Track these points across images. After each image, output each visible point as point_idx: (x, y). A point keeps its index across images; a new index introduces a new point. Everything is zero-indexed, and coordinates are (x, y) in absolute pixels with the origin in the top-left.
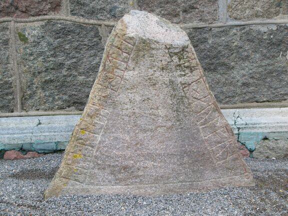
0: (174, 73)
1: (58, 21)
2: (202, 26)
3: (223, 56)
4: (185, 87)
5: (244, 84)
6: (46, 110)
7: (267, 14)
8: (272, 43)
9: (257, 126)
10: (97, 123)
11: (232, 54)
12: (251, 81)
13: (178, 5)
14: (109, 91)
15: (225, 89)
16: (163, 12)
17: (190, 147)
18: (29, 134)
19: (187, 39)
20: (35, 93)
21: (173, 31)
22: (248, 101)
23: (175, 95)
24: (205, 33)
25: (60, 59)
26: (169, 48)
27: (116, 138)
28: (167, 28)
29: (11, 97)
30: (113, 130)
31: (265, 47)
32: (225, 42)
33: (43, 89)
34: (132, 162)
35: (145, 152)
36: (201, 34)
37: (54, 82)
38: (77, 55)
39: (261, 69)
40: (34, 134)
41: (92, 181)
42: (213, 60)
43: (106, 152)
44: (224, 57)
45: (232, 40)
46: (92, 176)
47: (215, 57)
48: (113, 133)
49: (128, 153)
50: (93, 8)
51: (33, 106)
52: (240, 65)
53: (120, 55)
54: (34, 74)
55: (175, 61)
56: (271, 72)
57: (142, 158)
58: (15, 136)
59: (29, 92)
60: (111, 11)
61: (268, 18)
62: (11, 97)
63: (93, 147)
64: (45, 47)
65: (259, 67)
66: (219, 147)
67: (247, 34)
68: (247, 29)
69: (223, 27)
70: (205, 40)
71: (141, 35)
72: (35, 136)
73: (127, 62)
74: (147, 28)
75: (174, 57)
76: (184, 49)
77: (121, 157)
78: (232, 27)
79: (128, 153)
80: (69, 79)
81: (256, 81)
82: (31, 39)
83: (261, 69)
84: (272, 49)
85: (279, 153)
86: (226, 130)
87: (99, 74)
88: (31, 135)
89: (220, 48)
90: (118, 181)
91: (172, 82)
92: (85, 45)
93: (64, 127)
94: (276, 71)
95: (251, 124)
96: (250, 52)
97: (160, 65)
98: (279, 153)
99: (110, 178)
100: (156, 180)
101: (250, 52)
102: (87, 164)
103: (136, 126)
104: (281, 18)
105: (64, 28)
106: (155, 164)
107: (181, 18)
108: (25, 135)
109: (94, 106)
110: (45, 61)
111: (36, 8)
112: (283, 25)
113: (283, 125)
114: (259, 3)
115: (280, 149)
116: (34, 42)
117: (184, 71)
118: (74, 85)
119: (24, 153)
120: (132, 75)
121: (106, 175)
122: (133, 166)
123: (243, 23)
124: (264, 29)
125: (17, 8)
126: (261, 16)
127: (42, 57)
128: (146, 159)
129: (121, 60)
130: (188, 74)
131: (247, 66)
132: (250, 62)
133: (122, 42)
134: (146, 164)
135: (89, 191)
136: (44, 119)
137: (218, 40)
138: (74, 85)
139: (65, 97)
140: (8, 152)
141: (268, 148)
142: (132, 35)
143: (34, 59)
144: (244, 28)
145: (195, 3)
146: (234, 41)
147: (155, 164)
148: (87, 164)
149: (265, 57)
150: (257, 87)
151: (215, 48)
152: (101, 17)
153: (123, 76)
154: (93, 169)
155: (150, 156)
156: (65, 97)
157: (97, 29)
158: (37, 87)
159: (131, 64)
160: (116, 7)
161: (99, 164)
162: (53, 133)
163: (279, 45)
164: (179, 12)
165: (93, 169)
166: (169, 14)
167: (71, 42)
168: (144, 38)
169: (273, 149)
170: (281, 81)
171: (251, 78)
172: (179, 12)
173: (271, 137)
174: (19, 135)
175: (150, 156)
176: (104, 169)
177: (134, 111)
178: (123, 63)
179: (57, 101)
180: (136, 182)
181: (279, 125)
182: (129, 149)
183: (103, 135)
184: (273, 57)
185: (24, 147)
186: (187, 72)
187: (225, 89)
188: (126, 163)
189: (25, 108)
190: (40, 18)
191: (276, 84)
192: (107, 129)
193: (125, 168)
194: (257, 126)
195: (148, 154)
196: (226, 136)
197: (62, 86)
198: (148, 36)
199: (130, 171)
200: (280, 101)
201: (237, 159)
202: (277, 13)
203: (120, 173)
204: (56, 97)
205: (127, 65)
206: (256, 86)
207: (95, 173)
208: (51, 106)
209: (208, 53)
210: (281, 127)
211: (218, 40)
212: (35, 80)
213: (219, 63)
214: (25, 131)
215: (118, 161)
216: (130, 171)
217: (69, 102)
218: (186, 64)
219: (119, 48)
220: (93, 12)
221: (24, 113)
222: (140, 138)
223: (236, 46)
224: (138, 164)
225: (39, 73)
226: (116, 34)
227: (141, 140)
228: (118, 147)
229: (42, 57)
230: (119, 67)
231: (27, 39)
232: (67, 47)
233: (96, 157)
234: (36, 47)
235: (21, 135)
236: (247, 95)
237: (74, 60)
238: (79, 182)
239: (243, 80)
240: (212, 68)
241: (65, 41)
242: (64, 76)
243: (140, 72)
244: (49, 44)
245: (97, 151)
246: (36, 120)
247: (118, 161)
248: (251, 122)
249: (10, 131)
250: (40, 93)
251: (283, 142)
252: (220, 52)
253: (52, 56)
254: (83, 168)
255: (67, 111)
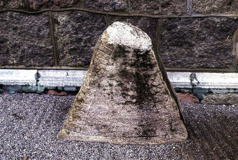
0: (140, 68)
1: (79, 12)
2: (174, 17)
3: (188, 37)
4: (147, 78)
5: (200, 56)
6: (72, 66)
7: (221, 10)
8: (222, 30)
9: (206, 84)
10: (88, 98)
11: (194, 36)
12: (205, 54)
13: (158, 2)
14: (96, 78)
15: (187, 59)
16: (147, 7)
17: (147, 115)
18: (60, 82)
19: (150, 45)
20: (65, 56)
21: (141, 38)
22: (202, 67)
23: (139, 82)
24: (176, 22)
25: (80, 35)
26: (137, 52)
27: (100, 108)
28: (138, 36)
29: (51, 58)
30: (98, 103)
31: (218, 32)
32: (190, 28)
33: (70, 53)
34: (109, 123)
35: (118, 117)
36: (173, 22)
37: (76, 49)
38: (90, 34)
39: (213, 47)
40: (64, 82)
41: (84, 132)
42: (180, 40)
43: (93, 116)
44: (188, 38)
45: (195, 27)
46: (85, 129)
47: (183, 37)
48: (98, 104)
49: (107, 117)
50: (101, 3)
51: (64, 63)
52: (199, 43)
53: (103, 55)
54: (64, 44)
55: (141, 60)
56: (220, 49)
57: (116, 121)
58: (54, 82)
59: (61, 55)
60: (112, 5)
61: (221, 13)
62: (51, 58)
63: (85, 112)
64: (70, 28)
65: (211, 45)
66: (167, 116)
67: (206, 23)
68: (206, 19)
69: (188, 18)
70: (176, 26)
71: (118, 43)
72: (65, 83)
73: (108, 60)
74: (123, 37)
75: (140, 58)
76: (147, 52)
77: (102, 119)
78: (195, 18)
79: (107, 117)
80: (85, 48)
81: (209, 55)
82: (62, 23)
83: (213, 47)
84: (222, 33)
85: (219, 102)
86: (172, 106)
87: (90, 66)
88: (62, 82)
89: (185, 32)
90: (100, 133)
91: (137, 74)
92: (96, 27)
93: (82, 78)
94: (223, 48)
95: (202, 83)
96: (207, 35)
97: (130, 62)
98: (219, 102)
99: (95, 131)
100: (124, 135)
101: (207, 35)
102: (82, 122)
103: (113, 100)
104: (230, 13)
105: (83, 16)
106: (124, 125)
107: (160, 11)
108: (58, 82)
109: (87, 87)
110: (70, 37)
111: (65, 3)
112: (232, 18)
113: (223, 85)
114: (215, 2)
115: (220, 100)
116: (63, 24)
117: (147, 67)
118: (89, 52)
119: (59, 92)
120: (111, 68)
121: (93, 129)
122: (110, 125)
123: (203, 16)
124: (217, 20)
125: (53, 3)
126: (217, 11)
127: (68, 35)
128: (118, 121)
129: (104, 58)
130: (149, 69)
131: (203, 45)
132: (205, 42)
133: (105, 47)
134: (118, 124)
135: (82, 138)
136: (70, 72)
137: (185, 27)
138: (89, 52)
139: (83, 59)
140: (50, 91)
141: (212, 99)
142: (111, 43)
143: (64, 35)
144: (204, 19)
145: (170, 1)
146: (195, 27)
147: (124, 125)
148: (82, 122)
149: (217, 39)
150: (209, 59)
151: (182, 32)
152: (106, 10)
153: (105, 68)
154: (85, 125)
155: (121, 120)
156: (83, 59)
157: (103, 17)
158: (66, 52)
159: (111, 61)
160: (115, 3)
161: (89, 123)
162: (75, 82)
163: (228, 31)
164: (159, 7)
165: (85, 125)
166: (152, 8)
167: (86, 25)
168: (120, 44)
169: (215, 100)
170: (226, 55)
171: (205, 52)
172: (159, 7)
173: (214, 91)
174: (56, 82)
175: (121, 120)
176: (92, 125)
177: (112, 91)
178: (105, 60)
179: (78, 61)
180: (111, 135)
181: (221, 84)
182: (108, 115)
183: (91, 105)
184: (223, 39)
185: (59, 89)
186: (148, 68)
187: (187, 59)
188: (105, 123)
189: (59, 64)
190: (67, 9)
191: (223, 57)
192: (94, 102)
193: (105, 126)
194: (206, 84)
195: (120, 118)
196: (172, 110)
197: (81, 52)
198: (123, 43)
199: (108, 128)
200: (224, 68)
201: (178, 124)
202: (228, 10)
203: (101, 128)
204: (78, 59)
205: (108, 62)
206: (209, 57)
207: (86, 128)
208: (75, 64)
209: (177, 35)
210: (222, 86)
211: (185, 27)
212: (65, 48)
213: (184, 42)
214: (59, 80)
215: (100, 121)
216: (108, 128)
217: (86, 62)
218: (148, 63)
219: (103, 51)
220: (101, 6)
221: (58, 67)
222: (115, 108)
223: (197, 31)
224: (113, 124)
225: (67, 44)
226: (101, 42)
227: (116, 109)
228: (101, 113)
229: (68, 35)
230: (103, 63)
231: (59, 23)
232: (84, 28)
233: (87, 118)
234: (65, 28)
235: (56, 82)
236: (202, 63)
237: (89, 37)
238: (77, 132)
239: (200, 53)
240: (180, 44)
241: (83, 24)
242: (82, 46)
243: (117, 66)
244: (73, 26)
245: (87, 115)
246: (65, 73)
247: (100, 121)
248: (202, 82)
249: (50, 79)
250: (68, 56)
251: (222, 95)
252: (185, 35)
253: (75, 34)
254: (79, 124)
255: (84, 68)
